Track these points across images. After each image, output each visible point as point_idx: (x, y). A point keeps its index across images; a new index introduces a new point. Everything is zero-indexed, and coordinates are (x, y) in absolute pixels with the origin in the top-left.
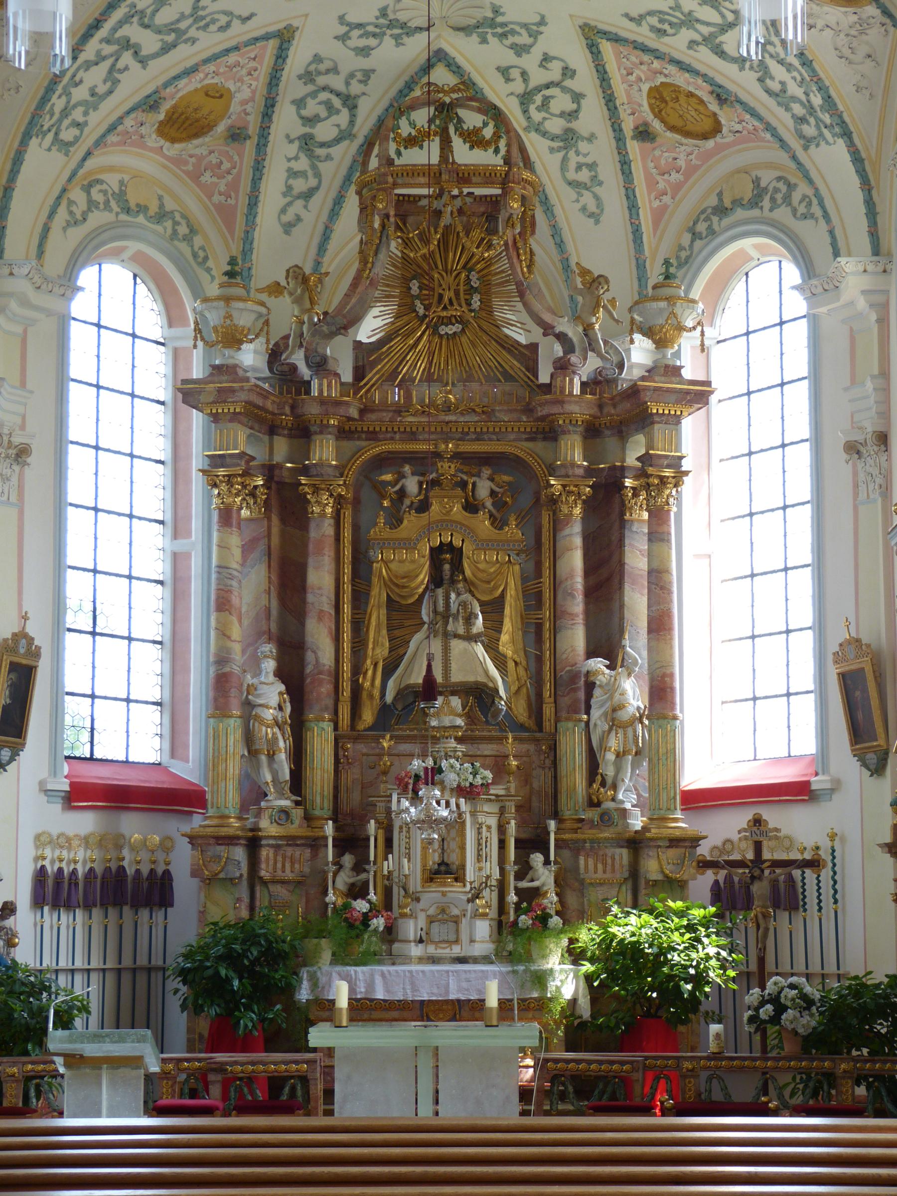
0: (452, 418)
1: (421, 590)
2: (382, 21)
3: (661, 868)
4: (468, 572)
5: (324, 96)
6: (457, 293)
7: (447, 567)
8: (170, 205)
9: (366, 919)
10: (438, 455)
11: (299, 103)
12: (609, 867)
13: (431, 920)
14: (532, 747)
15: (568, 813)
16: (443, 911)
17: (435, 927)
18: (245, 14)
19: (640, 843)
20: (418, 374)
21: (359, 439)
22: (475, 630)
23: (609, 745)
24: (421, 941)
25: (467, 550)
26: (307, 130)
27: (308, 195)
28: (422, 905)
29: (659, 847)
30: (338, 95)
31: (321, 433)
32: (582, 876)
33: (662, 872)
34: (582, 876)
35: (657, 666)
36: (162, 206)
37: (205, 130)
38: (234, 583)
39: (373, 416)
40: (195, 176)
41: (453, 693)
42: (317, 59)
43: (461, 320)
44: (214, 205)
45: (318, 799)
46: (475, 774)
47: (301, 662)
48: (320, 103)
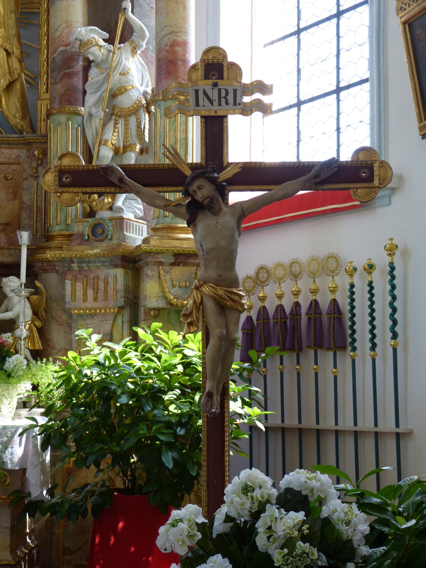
3: (163, 292)
12: (101, 294)
14: (23, 153)
15: (57, 228)
19: (140, 260)
23: (105, 137)
29: (161, 263)
32: (67, 306)
33: (165, 297)
34: (67, 306)
35: (164, 32)
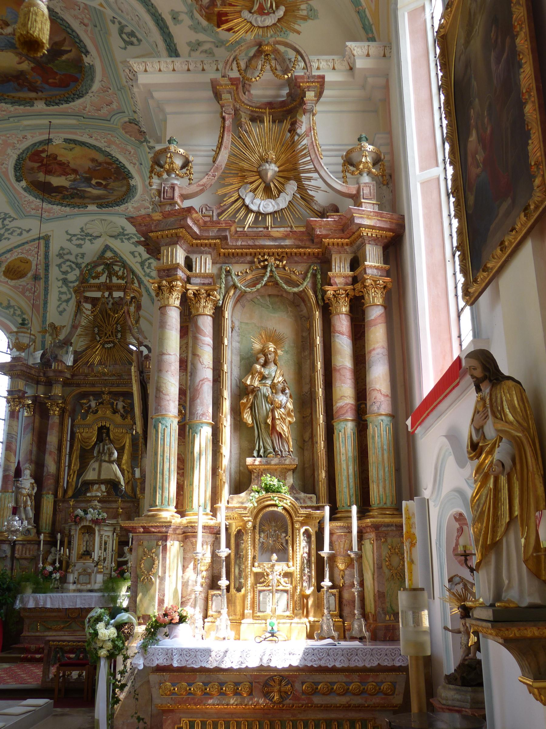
0: (107, 378)
1: (93, 444)
2: (82, 233)
4: (112, 437)
5: (68, 263)
6: (112, 332)
7: (104, 435)
8: (12, 303)
9: (51, 573)
10: (103, 393)
11: (59, 266)
13: (80, 574)
16: (85, 570)
17: (81, 577)
18: (27, 229)
20: (96, 362)
21: (73, 386)
22: (112, 459)
24: (74, 583)
25: (111, 428)
26: (64, 276)
27: (67, 301)
28: (76, 568)
30: (73, 263)
31: (55, 383)
36: (9, 303)
38: (14, 440)
39: (77, 378)
40: (23, 293)
41: (102, 483)
42: (62, 249)
43: (113, 342)
45: (44, 526)
46: (99, 514)
47: (42, 472)
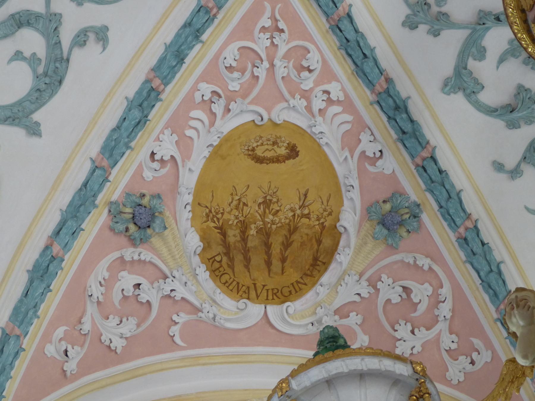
37: (327, 242)
44: (459, 386)
48: (502, 60)
